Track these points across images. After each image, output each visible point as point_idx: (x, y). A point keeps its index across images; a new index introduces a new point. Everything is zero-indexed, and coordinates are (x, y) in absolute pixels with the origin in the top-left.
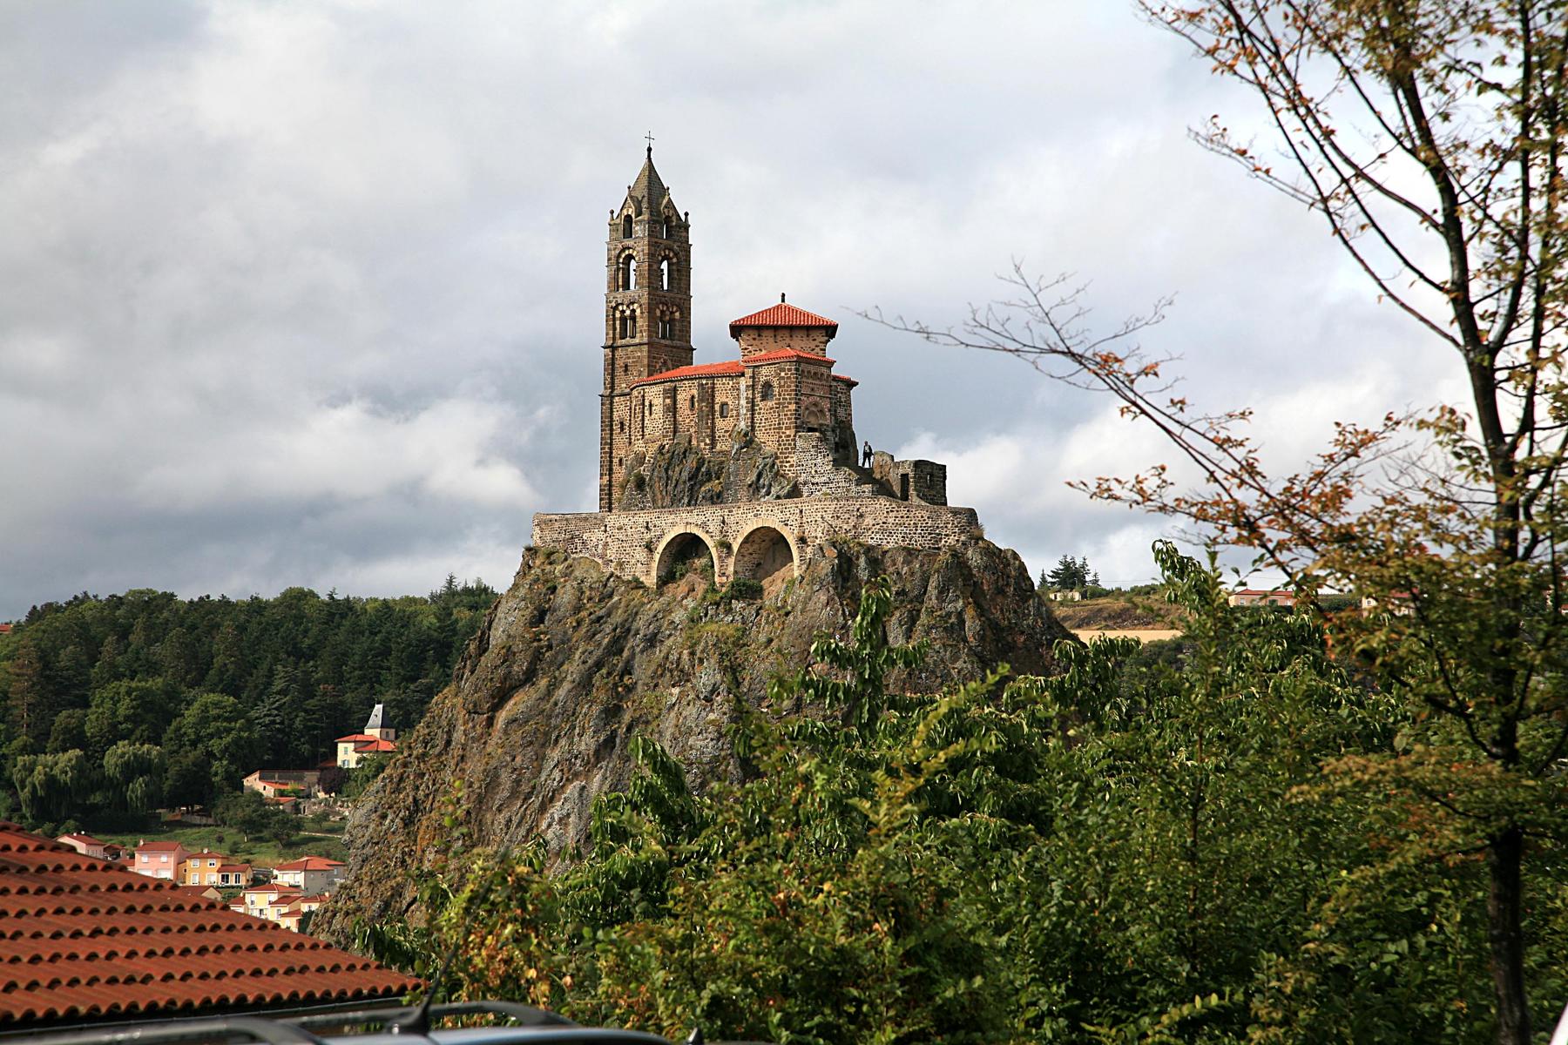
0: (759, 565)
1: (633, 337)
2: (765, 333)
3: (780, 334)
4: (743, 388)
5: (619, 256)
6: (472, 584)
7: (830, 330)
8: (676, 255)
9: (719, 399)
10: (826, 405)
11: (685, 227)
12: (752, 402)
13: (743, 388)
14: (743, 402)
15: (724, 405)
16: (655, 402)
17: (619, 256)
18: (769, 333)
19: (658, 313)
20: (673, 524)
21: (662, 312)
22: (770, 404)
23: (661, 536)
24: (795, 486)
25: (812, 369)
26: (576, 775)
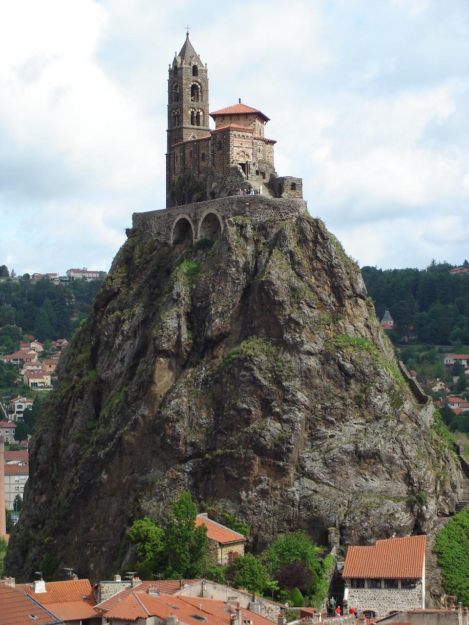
0: (215, 232)
1: (178, 125)
2: (226, 118)
3: (233, 118)
4: (210, 145)
5: (172, 86)
6: (442, 263)
7: (264, 119)
8: (200, 84)
9: (202, 151)
10: (250, 152)
11: (206, 71)
12: (213, 152)
13: (210, 145)
14: (210, 152)
15: (204, 154)
16: (179, 155)
17: (172, 86)
18: (228, 118)
19: (190, 113)
20: (178, 214)
21: (192, 112)
22: (220, 152)
23: (173, 221)
24: (230, 192)
25: (241, 134)
26: (129, 338)
